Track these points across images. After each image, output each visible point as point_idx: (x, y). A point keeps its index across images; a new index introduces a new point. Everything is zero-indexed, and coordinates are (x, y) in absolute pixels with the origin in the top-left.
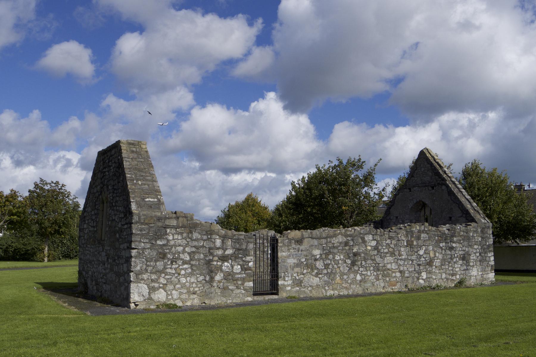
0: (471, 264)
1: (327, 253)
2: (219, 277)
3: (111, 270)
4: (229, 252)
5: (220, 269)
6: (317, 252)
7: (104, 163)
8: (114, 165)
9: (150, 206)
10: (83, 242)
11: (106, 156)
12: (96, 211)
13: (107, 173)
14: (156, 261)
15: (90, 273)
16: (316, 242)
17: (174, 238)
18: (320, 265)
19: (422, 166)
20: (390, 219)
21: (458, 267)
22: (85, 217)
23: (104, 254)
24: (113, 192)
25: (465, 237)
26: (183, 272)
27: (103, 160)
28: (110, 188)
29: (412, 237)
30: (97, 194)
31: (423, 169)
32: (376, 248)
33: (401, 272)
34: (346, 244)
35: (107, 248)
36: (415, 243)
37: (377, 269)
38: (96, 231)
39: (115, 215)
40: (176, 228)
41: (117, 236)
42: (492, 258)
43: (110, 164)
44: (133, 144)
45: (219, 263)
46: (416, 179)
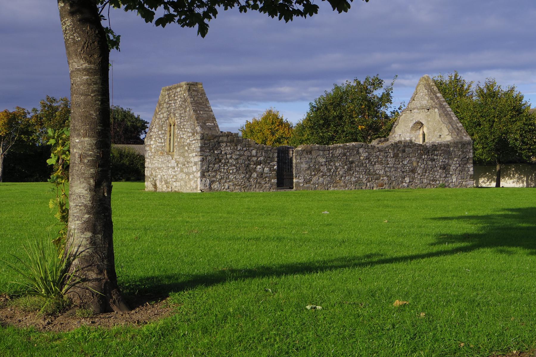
0: (451, 173)
1: (329, 161)
2: (255, 175)
3: (182, 171)
4: (262, 158)
5: (255, 170)
6: (322, 160)
7: (169, 97)
8: (180, 99)
9: (210, 129)
10: (150, 154)
11: (171, 91)
12: (163, 132)
14: (214, 164)
15: (159, 176)
16: (321, 153)
17: (226, 149)
18: (324, 169)
21: (439, 173)
23: (173, 161)
24: (181, 119)
25: (446, 151)
26: (231, 172)
27: (168, 94)
28: (177, 115)
29: (398, 150)
30: (164, 119)
31: (422, 94)
32: (367, 158)
33: (388, 177)
34: (345, 155)
35: (175, 157)
36: (400, 155)
37: (368, 173)
38: (164, 146)
39: (183, 134)
40: (227, 142)
41: (186, 148)
42: (472, 169)
43: (176, 98)
44: (193, 85)
45: (254, 166)
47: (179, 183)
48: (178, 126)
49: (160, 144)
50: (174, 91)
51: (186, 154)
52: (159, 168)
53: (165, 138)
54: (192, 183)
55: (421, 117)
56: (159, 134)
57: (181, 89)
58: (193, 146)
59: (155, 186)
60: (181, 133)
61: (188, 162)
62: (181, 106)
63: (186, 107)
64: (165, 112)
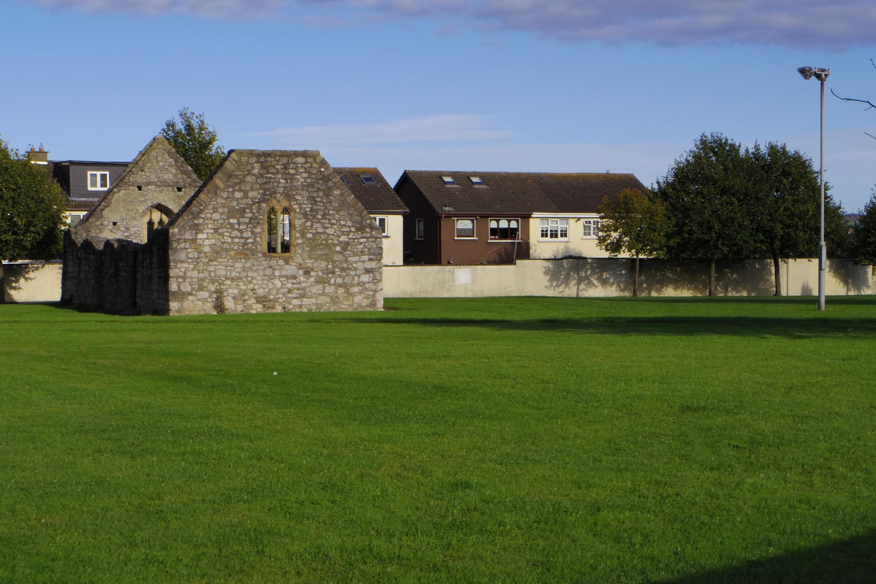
11: (269, 159)
13: (282, 181)
19: (159, 158)
20: (102, 224)
22: (198, 225)
28: (298, 197)
31: (161, 164)
38: (252, 243)
41: (338, 248)
46: (148, 174)
47: (314, 301)
48: (305, 215)
49: (237, 240)
50: (284, 160)
51: (338, 257)
52: (232, 279)
53: (258, 230)
54: (358, 299)
55: (165, 198)
56: (232, 225)
57: (309, 160)
58: (362, 246)
59: (220, 307)
60: (318, 225)
61: (343, 269)
62: (311, 185)
63: (329, 188)
64: (252, 189)
